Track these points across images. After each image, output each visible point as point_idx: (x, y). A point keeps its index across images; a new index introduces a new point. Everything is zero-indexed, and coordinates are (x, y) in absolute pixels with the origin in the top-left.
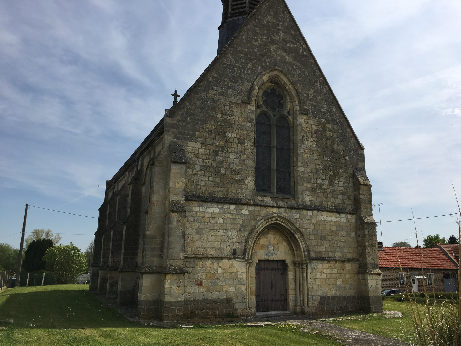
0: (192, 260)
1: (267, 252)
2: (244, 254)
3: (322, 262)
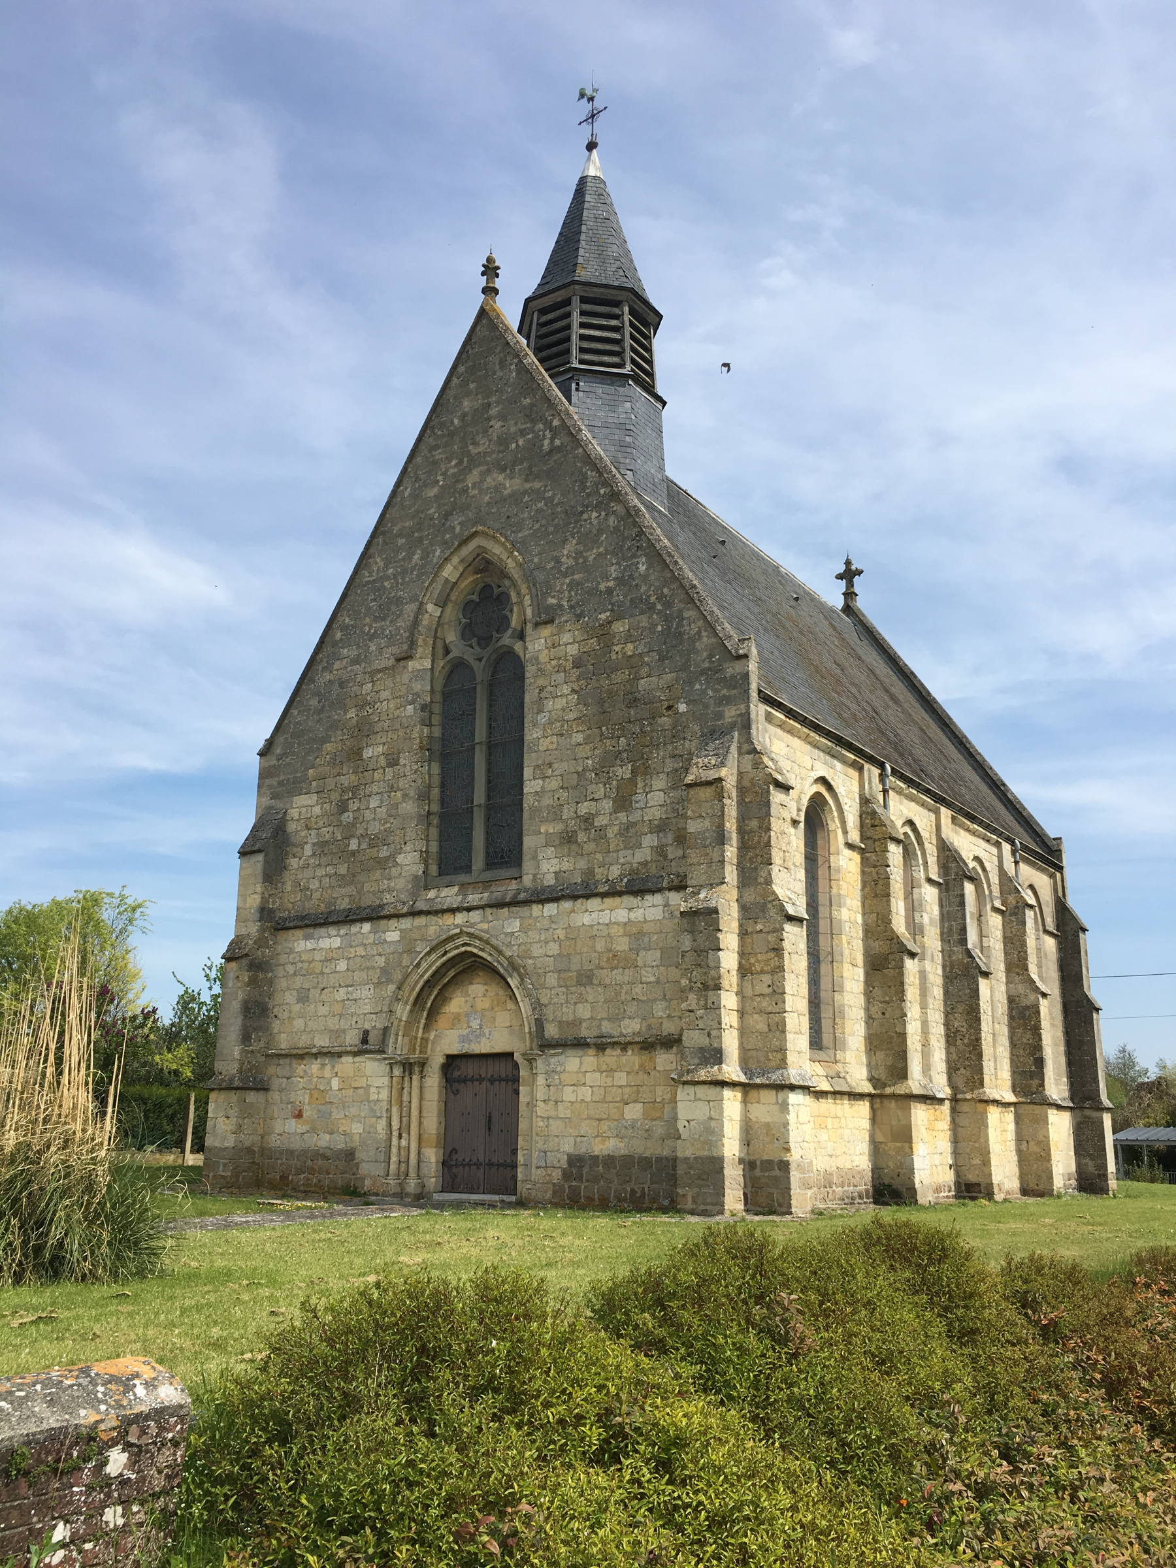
0: (287, 1061)
1: (465, 1032)
3: (581, 1053)
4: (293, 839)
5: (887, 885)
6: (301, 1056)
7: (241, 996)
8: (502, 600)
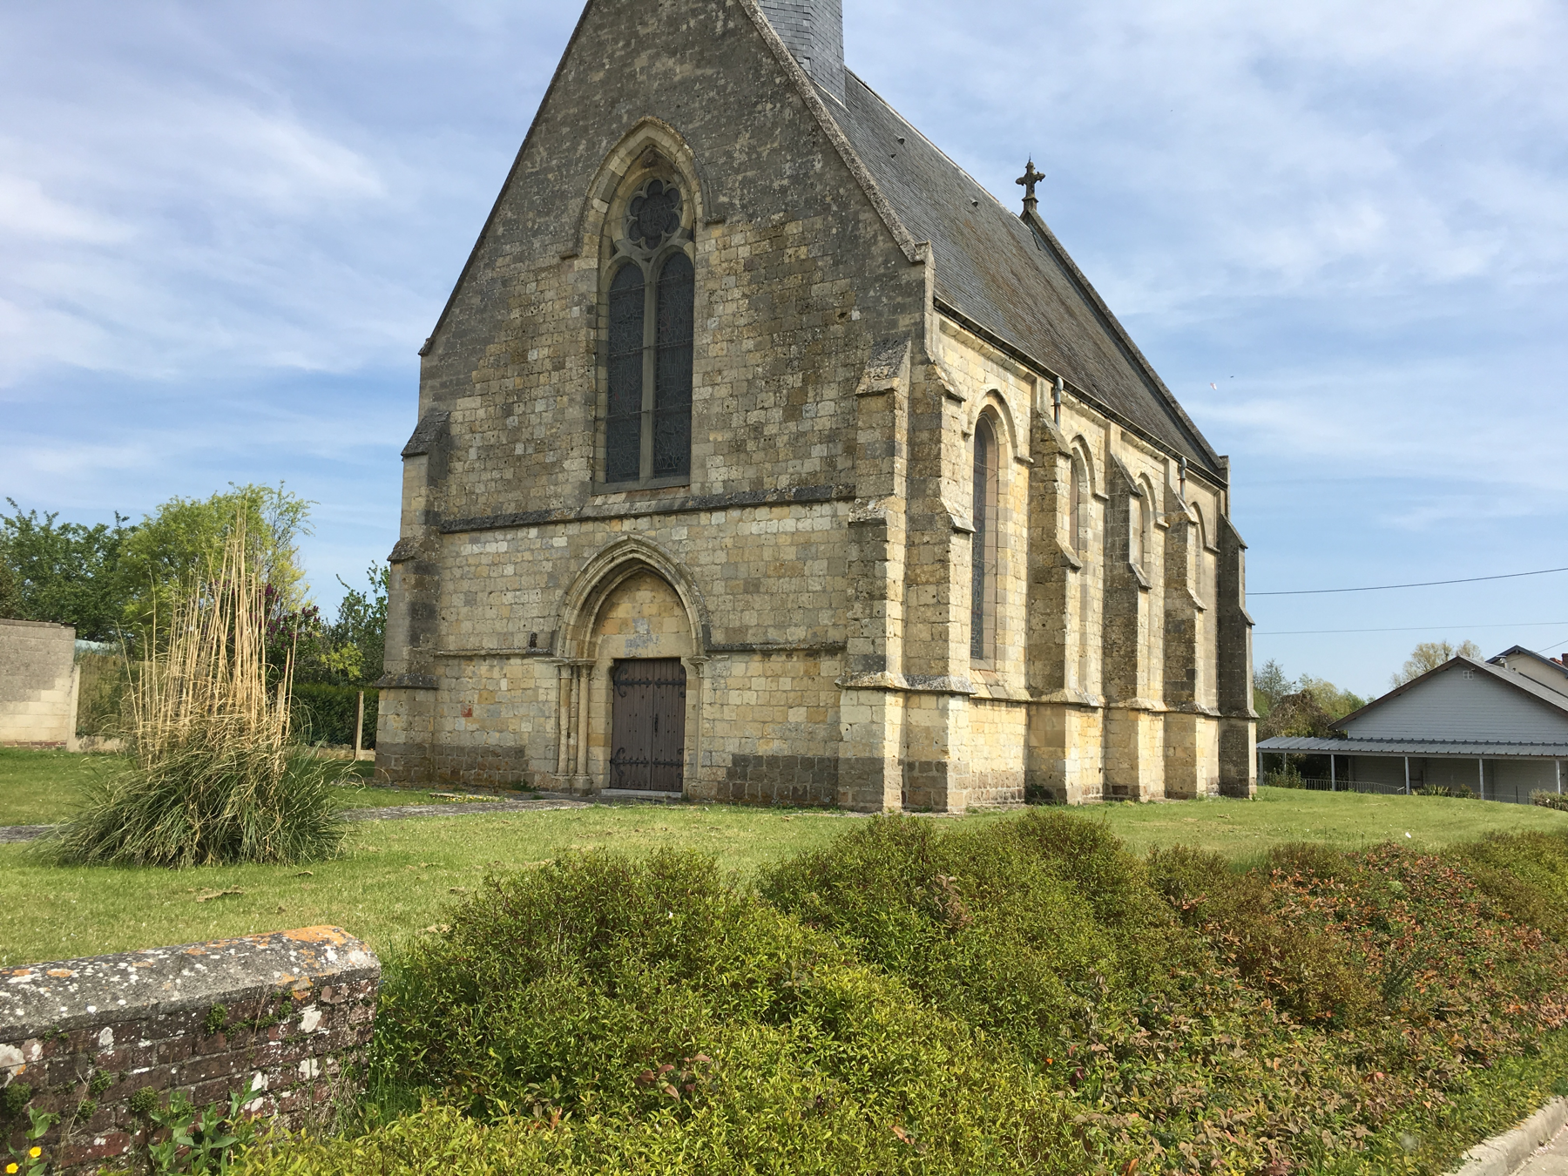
0: (456, 662)
1: (632, 637)
2: (552, 644)
4: (458, 442)
5: (1054, 500)
6: (470, 657)
7: (408, 597)
8: (672, 197)
